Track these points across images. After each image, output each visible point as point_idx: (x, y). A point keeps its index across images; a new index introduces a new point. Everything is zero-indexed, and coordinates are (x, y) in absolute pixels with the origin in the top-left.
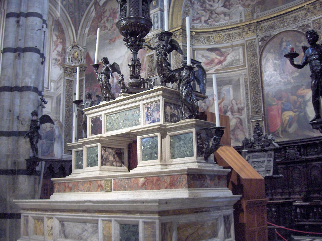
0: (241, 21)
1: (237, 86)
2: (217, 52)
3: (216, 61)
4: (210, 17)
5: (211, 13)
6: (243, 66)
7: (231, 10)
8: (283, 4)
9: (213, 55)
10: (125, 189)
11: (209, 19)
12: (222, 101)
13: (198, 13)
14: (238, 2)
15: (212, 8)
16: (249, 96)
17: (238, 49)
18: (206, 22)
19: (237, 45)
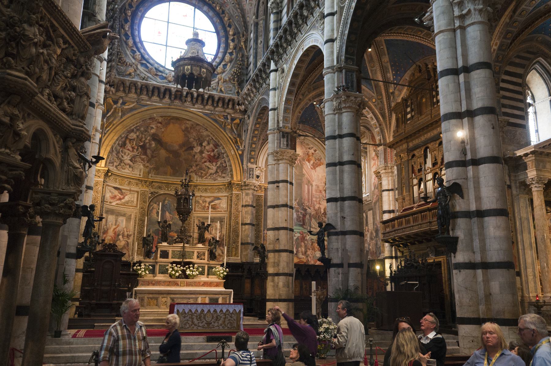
0: (140, 175)
1: (129, 219)
2: (119, 191)
3: (118, 197)
4: (119, 164)
5: (121, 162)
6: (135, 207)
7: (135, 165)
8: (170, 176)
9: (116, 193)
10: (192, 286)
11: (118, 165)
12: (117, 227)
13: (113, 159)
14: (141, 161)
15: (122, 158)
16: (136, 228)
17: (134, 194)
18: (116, 167)
19: (133, 191)
